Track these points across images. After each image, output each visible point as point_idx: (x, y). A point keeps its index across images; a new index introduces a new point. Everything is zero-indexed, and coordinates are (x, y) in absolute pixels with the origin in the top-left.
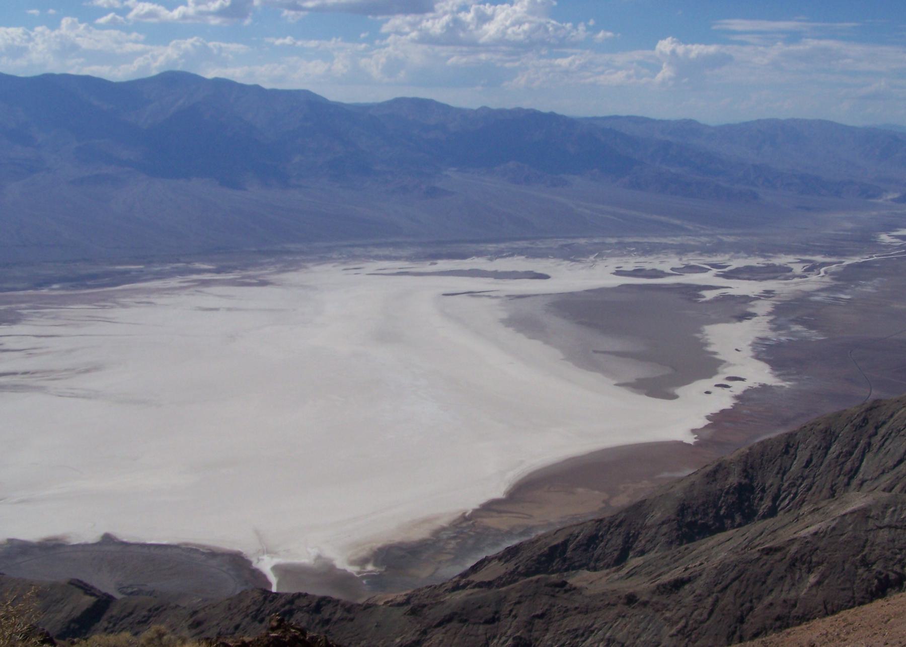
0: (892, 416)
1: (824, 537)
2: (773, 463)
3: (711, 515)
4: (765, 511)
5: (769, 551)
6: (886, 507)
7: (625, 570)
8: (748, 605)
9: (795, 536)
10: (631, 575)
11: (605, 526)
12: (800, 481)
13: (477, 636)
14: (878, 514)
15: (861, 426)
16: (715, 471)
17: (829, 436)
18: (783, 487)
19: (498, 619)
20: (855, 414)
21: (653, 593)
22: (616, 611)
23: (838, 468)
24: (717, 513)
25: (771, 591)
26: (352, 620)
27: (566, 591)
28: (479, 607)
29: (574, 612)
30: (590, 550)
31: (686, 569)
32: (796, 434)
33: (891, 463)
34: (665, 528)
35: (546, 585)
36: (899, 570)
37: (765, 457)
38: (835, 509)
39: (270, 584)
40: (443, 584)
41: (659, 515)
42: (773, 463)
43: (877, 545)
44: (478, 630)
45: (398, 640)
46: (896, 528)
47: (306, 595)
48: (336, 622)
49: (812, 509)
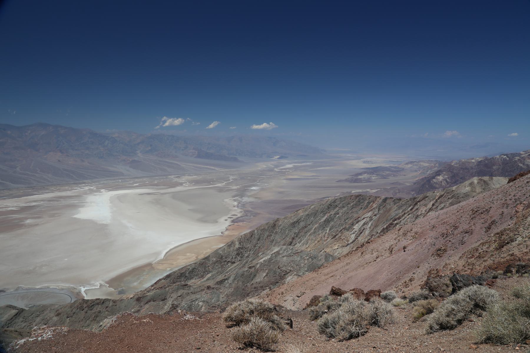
3: (231, 258)
5: (250, 268)
6: (285, 250)
7: (205, 279)
8: (246, 285)
9: (258, 262)
10: (208, 280)
12: (257, 245)
13: (160, 306)
16: (231, 244)
19: (166, 299)
21: (215, 284)
22: (205, 292)
25: (252, 280)
26: (116, 305)
27: (188, 287)
28: (160, 296)
29: (191, 294)
30: (193, 273)
31: (225, 276)
34: (217, 264)
35: (181, 286)
36: (290, 269)
38: (269, 253)
39: (84, 297)
40: (146, 289)
41: (215, 259)
44: (160, 303)
45: (133, 310)
46: (288, 256)
47: (99, 299)
48: (110, 307)
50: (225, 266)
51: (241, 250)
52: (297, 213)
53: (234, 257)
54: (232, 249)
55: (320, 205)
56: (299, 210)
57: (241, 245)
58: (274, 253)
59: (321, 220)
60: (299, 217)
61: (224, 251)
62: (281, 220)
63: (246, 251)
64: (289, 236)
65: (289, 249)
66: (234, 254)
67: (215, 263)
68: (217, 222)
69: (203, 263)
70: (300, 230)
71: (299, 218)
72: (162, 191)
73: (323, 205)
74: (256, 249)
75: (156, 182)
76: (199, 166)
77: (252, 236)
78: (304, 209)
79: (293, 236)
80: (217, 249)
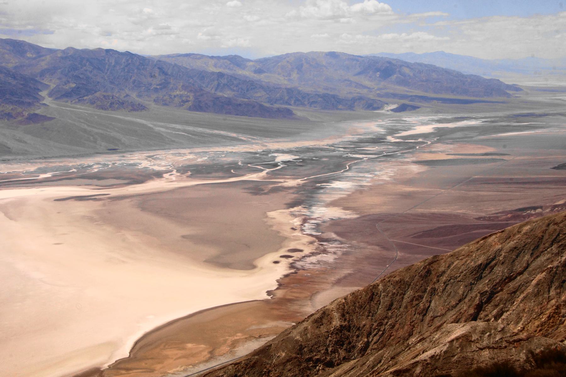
0: (449, 267)
1: (439, 358)
2: (364, 309)
3: (323, 352)
4: (362, 345)
6: (483, 332)
9: (417, 359)
11: (242, 368)
12: (386, 321)
14: (477, 339)
15: (426, 276)
16: (321, 318)
17: (402, 285)
18: (374, 327)
20: (421, 268)
23: (414, 309)
24: (327, 350)
32: (378, 285)
33: (453, 303)
34: (289, 367)
37: (357, 305)
41: (284, 354)
42: (364, 309)
43: (481, 362)
49: (419, 339)
50: (309, 372)
51: (347, 333)
52: (485, 242)
53: (330, 349)
54: (323, 329)
55: (548, 225)
56: (490, 236)
57: (345, 320)
58: (457, 339)
59: (552, 261)
60: (491, 253)
61: (306, 334)
62: (443, 261)
63: (358, 336)
64: (466, 300)
65: (495, 329)
66: (330, 341)
67: (284, 364)
68: (254, 267)
69: (255, 363)
70: (495, 285)
71: (491, 257)
72: (114, 192)
73: (556, 224)
74: (384, 329)
75: (96, 170)
76: (200, 130)
77: (371, 299)
78: (504, 235)
79: (477, 301)
80: (286, 330)
